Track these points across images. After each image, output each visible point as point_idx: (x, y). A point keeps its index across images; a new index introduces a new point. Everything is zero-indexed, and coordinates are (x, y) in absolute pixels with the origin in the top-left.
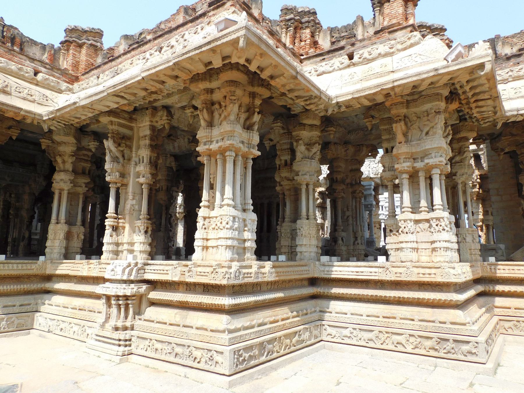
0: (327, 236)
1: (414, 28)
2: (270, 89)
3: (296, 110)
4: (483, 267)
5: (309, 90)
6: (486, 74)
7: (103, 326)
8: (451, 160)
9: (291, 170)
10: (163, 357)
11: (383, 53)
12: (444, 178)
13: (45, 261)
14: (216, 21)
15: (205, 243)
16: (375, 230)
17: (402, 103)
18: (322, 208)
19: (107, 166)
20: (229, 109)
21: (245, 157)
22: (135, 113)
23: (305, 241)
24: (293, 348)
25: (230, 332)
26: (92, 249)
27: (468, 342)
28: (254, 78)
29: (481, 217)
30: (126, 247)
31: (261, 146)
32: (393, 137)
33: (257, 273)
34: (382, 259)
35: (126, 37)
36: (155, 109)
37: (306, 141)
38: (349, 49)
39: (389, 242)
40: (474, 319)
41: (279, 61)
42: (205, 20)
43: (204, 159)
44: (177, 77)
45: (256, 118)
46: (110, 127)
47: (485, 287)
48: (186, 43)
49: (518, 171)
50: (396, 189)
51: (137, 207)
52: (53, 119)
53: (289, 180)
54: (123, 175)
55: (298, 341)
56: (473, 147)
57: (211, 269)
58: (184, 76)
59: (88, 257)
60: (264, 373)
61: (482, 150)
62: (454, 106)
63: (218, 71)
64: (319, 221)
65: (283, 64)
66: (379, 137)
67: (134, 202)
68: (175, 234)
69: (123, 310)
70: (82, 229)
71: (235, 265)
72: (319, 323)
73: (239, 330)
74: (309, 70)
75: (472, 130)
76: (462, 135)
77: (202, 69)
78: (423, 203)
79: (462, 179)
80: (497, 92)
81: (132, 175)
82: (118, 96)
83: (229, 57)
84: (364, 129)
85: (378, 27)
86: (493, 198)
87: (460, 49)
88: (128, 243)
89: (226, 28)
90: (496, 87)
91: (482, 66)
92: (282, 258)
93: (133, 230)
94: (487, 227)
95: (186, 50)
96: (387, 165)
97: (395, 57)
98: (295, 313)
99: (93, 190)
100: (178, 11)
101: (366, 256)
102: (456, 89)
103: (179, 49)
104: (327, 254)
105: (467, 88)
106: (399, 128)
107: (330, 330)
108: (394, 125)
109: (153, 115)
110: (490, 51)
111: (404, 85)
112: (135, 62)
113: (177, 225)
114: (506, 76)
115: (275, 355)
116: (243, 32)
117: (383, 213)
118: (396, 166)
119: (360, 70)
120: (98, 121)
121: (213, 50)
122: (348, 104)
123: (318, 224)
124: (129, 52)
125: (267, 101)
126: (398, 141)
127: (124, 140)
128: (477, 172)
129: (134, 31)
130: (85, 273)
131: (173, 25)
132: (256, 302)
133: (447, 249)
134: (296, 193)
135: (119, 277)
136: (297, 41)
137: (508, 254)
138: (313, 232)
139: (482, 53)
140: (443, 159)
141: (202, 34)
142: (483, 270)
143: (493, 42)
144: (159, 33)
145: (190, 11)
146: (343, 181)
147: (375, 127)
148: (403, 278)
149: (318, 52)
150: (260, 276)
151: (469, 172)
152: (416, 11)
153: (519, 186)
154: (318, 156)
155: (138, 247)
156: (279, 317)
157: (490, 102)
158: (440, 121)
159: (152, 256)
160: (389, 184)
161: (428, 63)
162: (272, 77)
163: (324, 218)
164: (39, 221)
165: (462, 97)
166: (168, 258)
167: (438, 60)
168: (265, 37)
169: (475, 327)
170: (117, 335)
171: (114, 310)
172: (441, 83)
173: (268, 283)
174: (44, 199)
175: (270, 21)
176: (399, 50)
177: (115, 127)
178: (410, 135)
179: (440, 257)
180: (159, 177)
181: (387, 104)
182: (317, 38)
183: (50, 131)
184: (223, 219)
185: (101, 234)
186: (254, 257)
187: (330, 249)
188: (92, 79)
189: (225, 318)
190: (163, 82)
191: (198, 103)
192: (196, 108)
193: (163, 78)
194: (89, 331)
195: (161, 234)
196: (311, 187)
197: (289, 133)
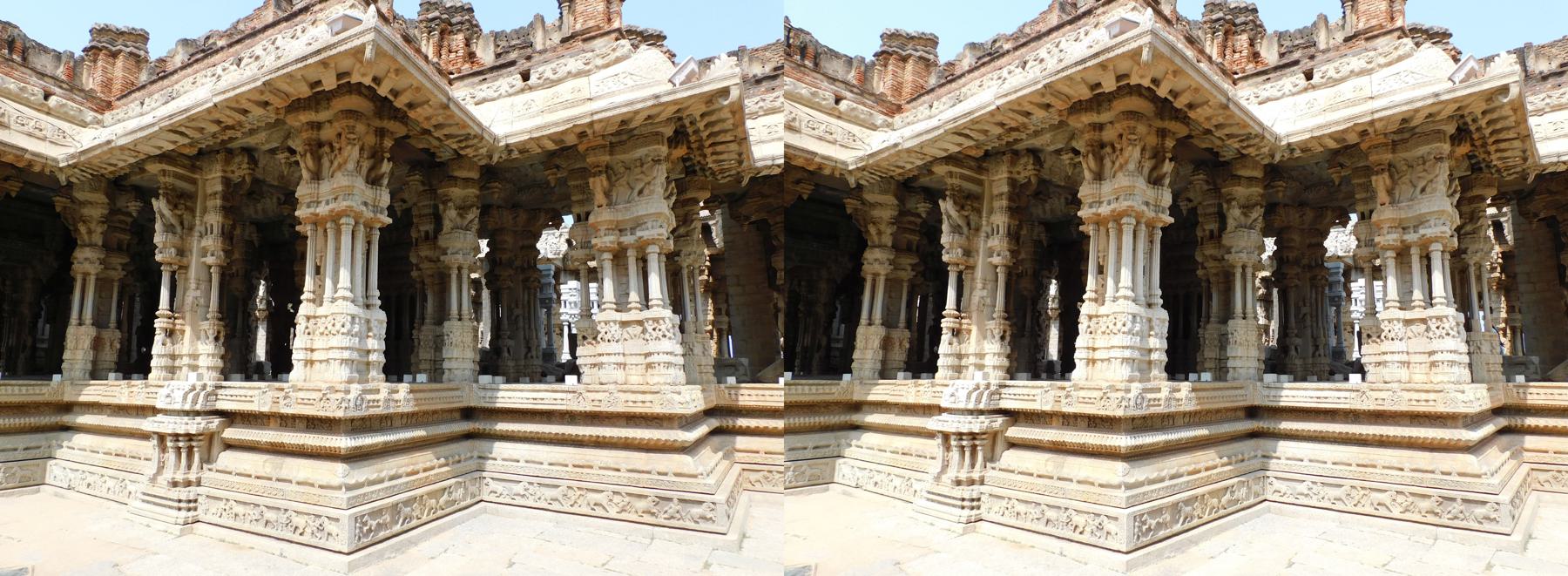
0: (1273, 343)
1: (1403, 32)
2: (1187, 125)
3: (1228, 155)
4: (1506, 390)
5: (1246, 126)
6: (1512, 102)
7: (938, 478)
8: (1458, 229)
9: (1220, 245)
10: (1028, 525)
11: (1357, 70)
12: (1448, 256)
13: (851, 382)
14: (1108, 22)
15: (1091, 355)
16: (1345, 335)
17: (1386, 145)
18: (1266, 301)
19: (945, 240)
20: (1126, 154)
21: (1151, 226)
22: (983, 160)
23: (1240, 351)
24: (1222, 512)
25: (1129, 487)
26: (922, 363)
27: (1484, 503)
28: (1164, 108)
29: (1504, 315)
30: (972, 360)
31: (1174, 210)
32: (1372, 196)
33: (1168, 399)
34: (1355, 378)
35: (973, 46)
36: (1016, 153)
37: (1243, 201)
38: (1306, 64)
39: (1367, 353)
40: (1493, 469)
41: (1202, 81)
42: (1091, 20)
43: (1089, 229)
44: (1048, 106)
45: (1168, 167)
46: (949, 181)
47: (1511, 421)
48: (1062, 55)
49: (1559, 248)
50: (1377, 273)
51: (988, 301)
52: (863, 169)
53: (1216, 259)
54: (968, 253)
55: (1229, 501)
56: (1492, 211)
57: (1100, 394)
58: (1059, 105)
59: (916, 376)
60: (1179, 549)
61: (1505, 215)
62: (1464, 149)
63: (1110, 97)
64: (1262, 321)
65: (1207, 86)
66: (1351, 195)
67: (985, 293)
68: (1046, 342)
69: (967, 454)
70: (907, 334)
71: (1136, 387)
72: (1261, 474)
73: (1141, 484)
74: (1246, 95)
75: (1489, 185)
76: (1476, 192)
77: (1086, 94)
78: (1417, 295)
79: (1476, 258)
80: (1528, 128)
81: (982, 254)
82: (960, 134)
83: (1126, 76)
84: (1328, 183)
85: (1349, 32)
86: (1522, 288)
87: (1472, 64)
88: (976, 355)
89: (1122, 33)
90: (1526, 121)
91: (1505, 90)
92: (1206, 376)
93: (983, 335)
94: (1513, 330)
95: (1063, 65)
96: (1362, 237)
97: (1376, 77)
98: (1225, 459)
99: (924, 275)
100: (1051, 8)
101: (1332, 373)
102: (1466, 124)
103: (1052, 64)
104: (1272, 372)
105: (1483, 123)
106: (1380, 182)
107: (1277, 485)
108: (1374, 178)
109: (1013, 163)
110: (1518, 67)
111: (1389, 117)
112: (986, 83)
113: (1048, 327)
114: (1541, 105)
115: (1196, 522)
116: (1147, 39)
117: (1357, 310)
118: (1377, 239)
119: (1322, 96)
120: (931, 172)
121: (1103, 66)
122: (1305, 147)
123: (1259, 327)
124: (977, 68)
125: (1183, 142)
126: (1379, 201)
127: (970, 201)
128: (1497, 249)
129: (984, 37)
130: (911, 400)
131: (1043, 28)
132: (1167, 442)
133: (1452, 363)
134: (1227, 279)
135: (962, 406)
136: (1228, 52)
137: (1544, 371)
138: (1253, 337)
139: (1505, 70)
140: (1446, 229)
141: (1086, 41)
142: (1506, 395)
143: (1521, 54)
144: (1023, 41)
145: (1068, 8)
146: (1297, 262)
147: (1345, 180)
148: (1387, 407)
149: (1260, 68)
150: (1173, 403)
151: (1486, 248)
152: (1406, 7)
153: (1561, 269)
154: (1260, 225)
155: (990, 361)
156: (1202, 465)
157: (1517, 144)
158: (1443, 171)
159: (1012, 373)
160: (1366, 265)
161: (1425, 84)
162: (1191, 106)
163: (1268, 317)
164: (842, 321)
165: (1476, 136)
166: (1036, 377)
167: (1440, 81)
168: (1181, 45)
169: (1496, 480)
170: (959, 492)
171: (955, 455)
172: (1444, 115)
173: (1185, 414)
174: (850, 289)
175: (1189, 22)
176: (1380, 66)
177: (956, 181)
178: (1397, 193)
179: (1442, 376)
180: (1023, 256)
181: (1364, 146)
182: (1258, 47)
183: (859, 187)
184: (1118, 320)
185: (936, 341)
186: (1165, 375)
187: (1277, 362)
188: (921, 108)
189: (1120, 466)
190: (1028, 114)
191: (1079, 145)
192: (1077, 153)
193: (1028, 108)
194: (917, 486)
195: (1025, 341)
196: (1249, 271)
197: (1217, 190)
